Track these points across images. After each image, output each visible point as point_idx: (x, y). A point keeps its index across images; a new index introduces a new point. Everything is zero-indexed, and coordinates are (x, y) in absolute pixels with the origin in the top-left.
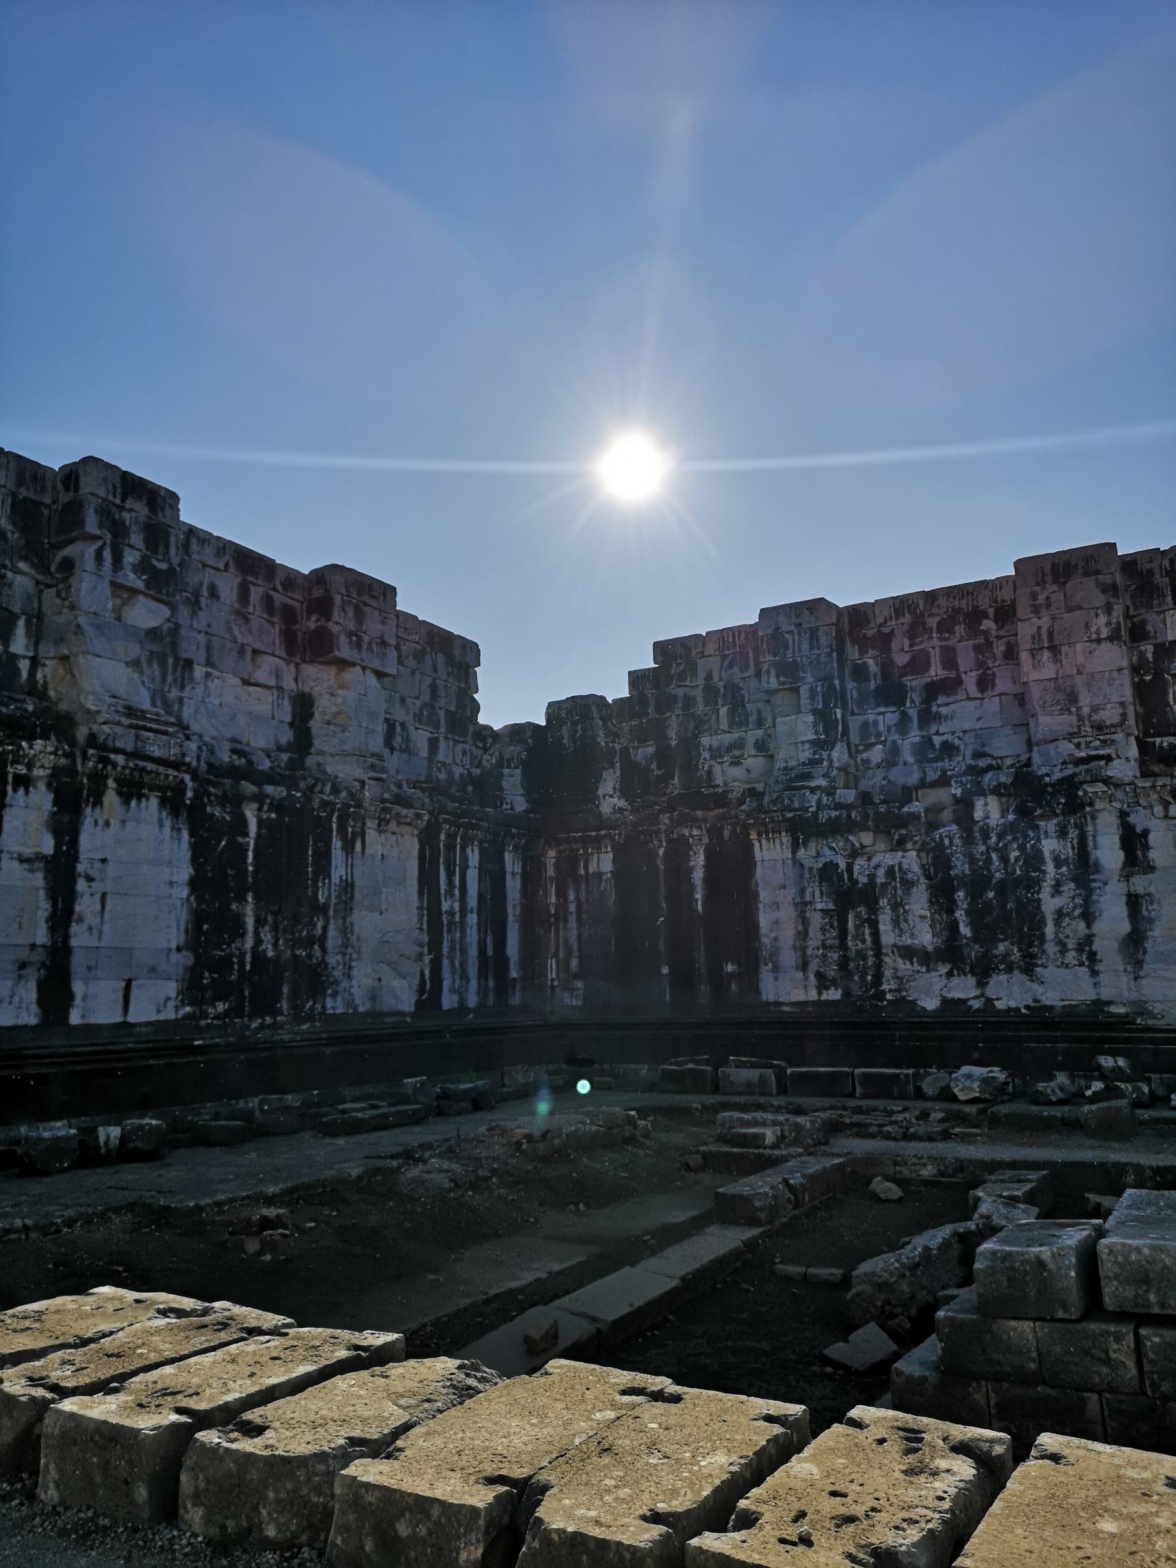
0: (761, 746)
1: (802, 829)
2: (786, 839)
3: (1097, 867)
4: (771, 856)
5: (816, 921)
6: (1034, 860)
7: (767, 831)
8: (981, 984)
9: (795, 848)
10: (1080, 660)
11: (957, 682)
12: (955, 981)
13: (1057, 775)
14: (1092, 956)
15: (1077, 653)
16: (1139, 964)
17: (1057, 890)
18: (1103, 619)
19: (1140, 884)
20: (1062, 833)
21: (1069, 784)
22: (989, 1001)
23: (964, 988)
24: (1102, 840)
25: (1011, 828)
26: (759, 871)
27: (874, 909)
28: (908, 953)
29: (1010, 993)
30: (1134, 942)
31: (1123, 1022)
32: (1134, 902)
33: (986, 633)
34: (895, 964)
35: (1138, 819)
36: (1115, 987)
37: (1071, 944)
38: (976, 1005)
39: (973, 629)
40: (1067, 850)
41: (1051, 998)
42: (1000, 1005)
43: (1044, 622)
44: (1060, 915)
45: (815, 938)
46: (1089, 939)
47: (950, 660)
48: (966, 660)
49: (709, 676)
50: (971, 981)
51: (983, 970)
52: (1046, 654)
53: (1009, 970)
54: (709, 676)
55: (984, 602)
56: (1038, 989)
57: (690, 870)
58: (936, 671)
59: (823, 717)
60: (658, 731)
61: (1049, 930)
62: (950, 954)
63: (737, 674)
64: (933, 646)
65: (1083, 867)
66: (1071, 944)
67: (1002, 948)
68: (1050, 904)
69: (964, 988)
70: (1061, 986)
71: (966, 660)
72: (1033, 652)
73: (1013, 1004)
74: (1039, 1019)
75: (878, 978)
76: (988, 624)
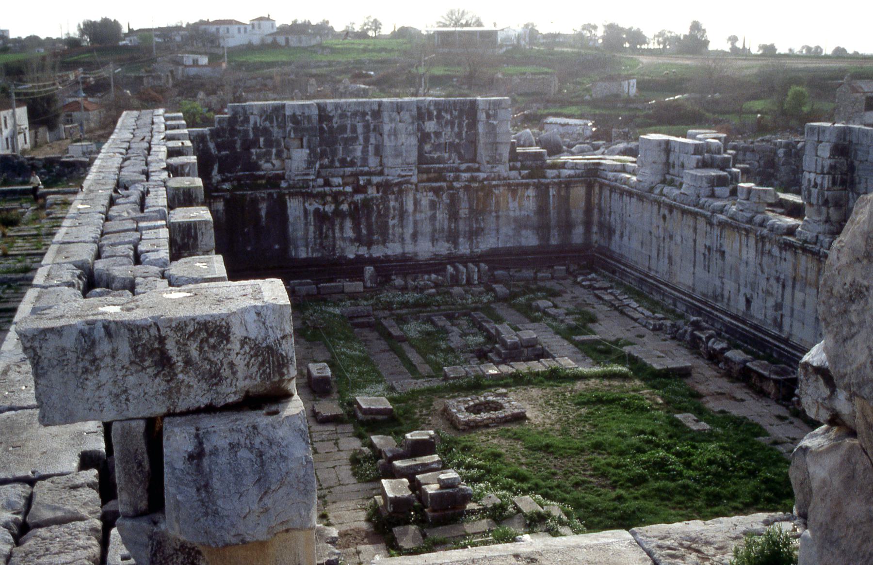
0: (279, 155)
1: (307, 196)
2: (301, 200)
3: (406, 211)
4: (294, 207)
5: (312, 228)
6: (387, 209)
7: (292, 195)
8: (369, 249)
9: (304, 203)
10: (404, 141)
11: (357, 138)
12: (360, 248)
13: (396, 181)
14: (403, 239)
15: (402, 138)
16: (416, 241)
17: (393, 218)
18: (411, 127)
19: (418, 216)
20: (396, 200)
21: (399, 184)
22: (371, 255)
23: (363, 251)
24: (409, 203)
25: (381, 197)
26: (289, 211)
27: (333, 225)
28: (344, 239)
29: (377, 252)
30: (414, 236)
31: (411, 259)
32: (415, 223)
33: (368, 121)
34: (339, 243)
35: (418, 196)
36: (410, 248)
37: (397, 235)
38: (367, 256)
39: (364, 120)
40: (397, 205)
41: (390, 253)
42: (374, 256)
43: (393, 125)
44: (394, 226)
45: (311, 235)
46: (403, 234)
47: (354, 129)
48: (360, 129)
49: (256, 123)
50: (366, 248)
51: (369, 244)
52: (393, 137)
53: (378, 244)
54: (256, 123)
55: (367, 109)
56: (386, 250)
57: (260, 210)
58: (348, 134)
59: (312, 151)
60: (231, 146)
61: (391, 232)
62: (358, 240)
63: (267, 124)
64: (348, 122)
65: (402, 214)
66: (397, 235)
67: (375, 237)
68: (391, 222)
69: (363, 251)
70: (394, 249)
71: (360, 129)
72: (389, 136)
73: (378, 255)
74: (387, 259)
75: (334, 250)
76: (368, 118)
